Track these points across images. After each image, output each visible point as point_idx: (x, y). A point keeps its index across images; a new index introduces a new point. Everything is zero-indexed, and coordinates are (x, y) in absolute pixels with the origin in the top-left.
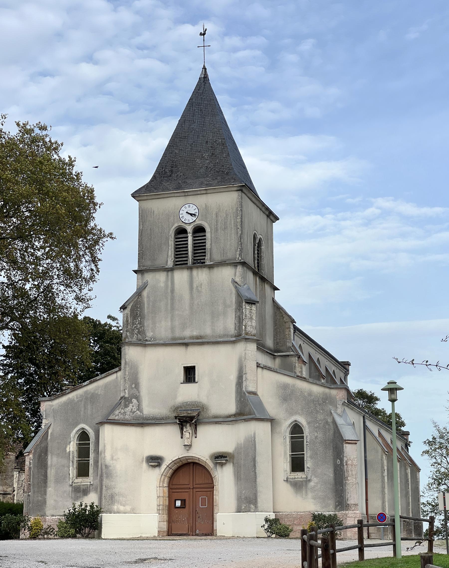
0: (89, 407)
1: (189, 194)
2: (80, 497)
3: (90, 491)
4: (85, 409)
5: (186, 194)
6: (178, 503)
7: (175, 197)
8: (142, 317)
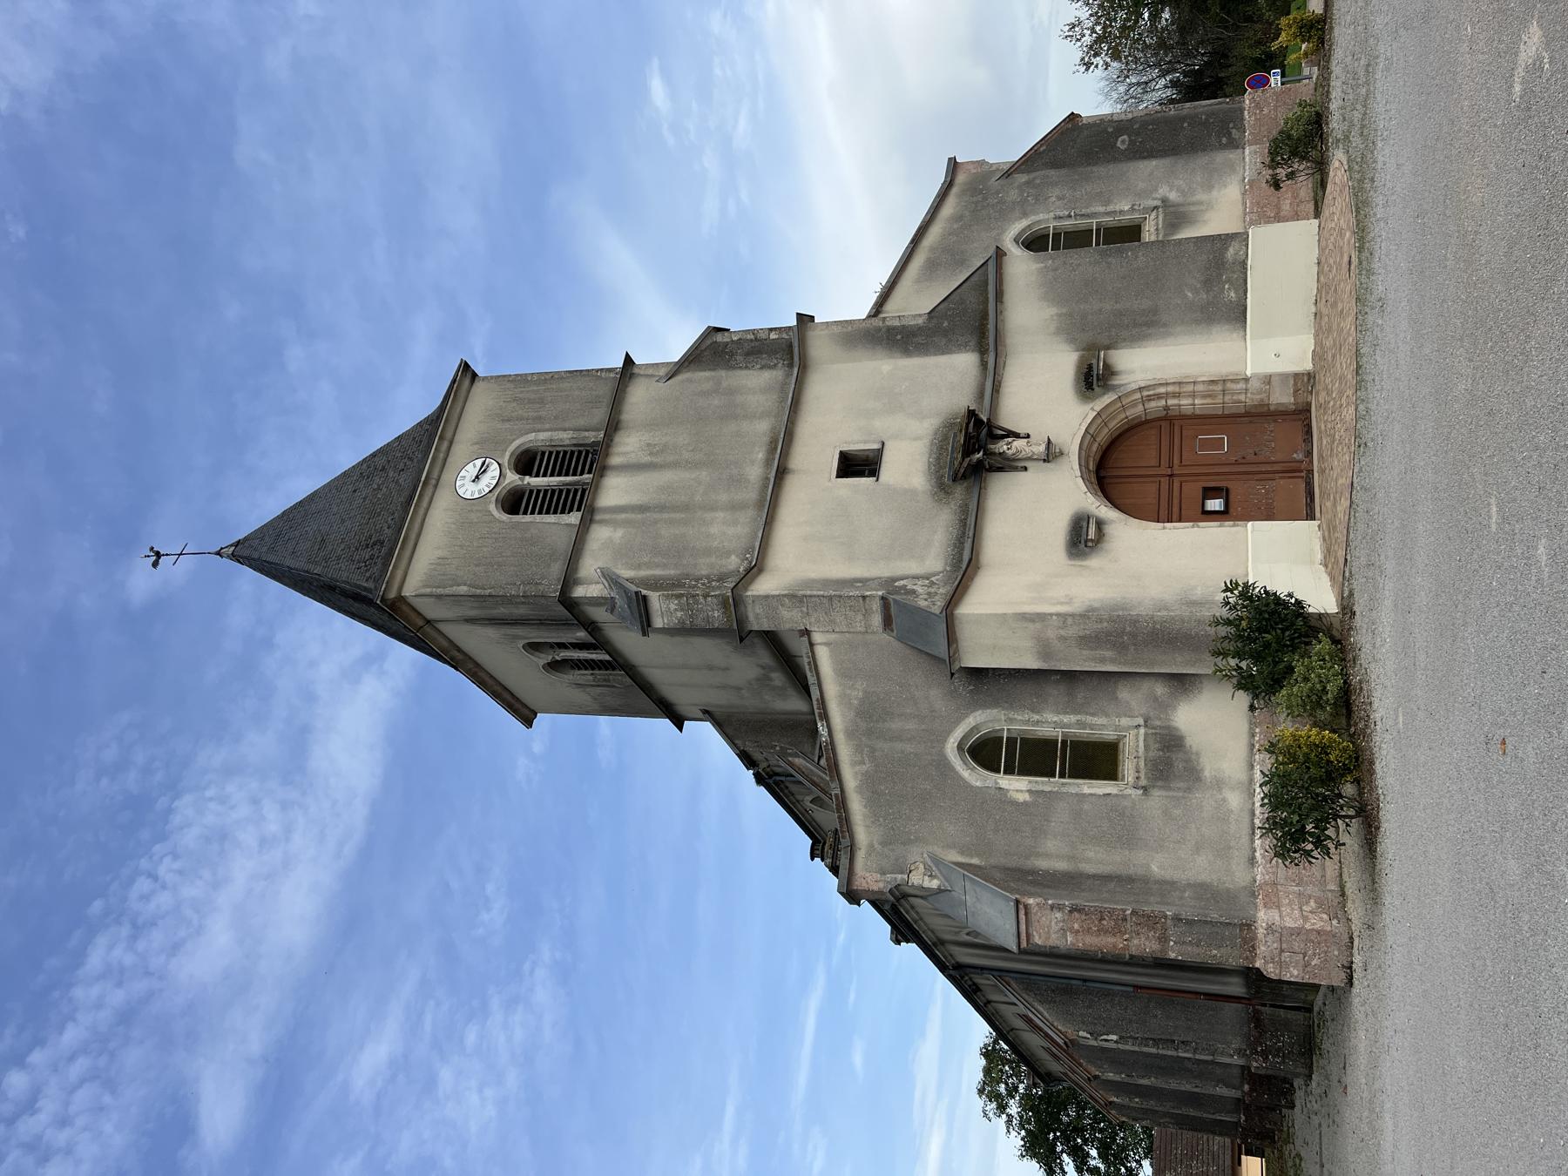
0: (896, 725)
1: (435, 474)
2: (1188, 761)
3: (1168, 727)
4: (897, 737)
6: (1215, 504)
7: (427, 510)
8: (687, 576)
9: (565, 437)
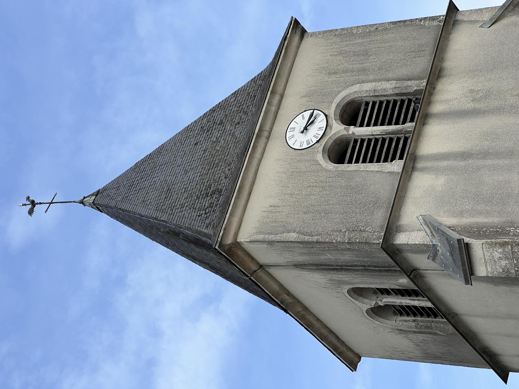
1: (267, 127)
5: (266, 134)
7: (260, 160)
9: (387, 88)
